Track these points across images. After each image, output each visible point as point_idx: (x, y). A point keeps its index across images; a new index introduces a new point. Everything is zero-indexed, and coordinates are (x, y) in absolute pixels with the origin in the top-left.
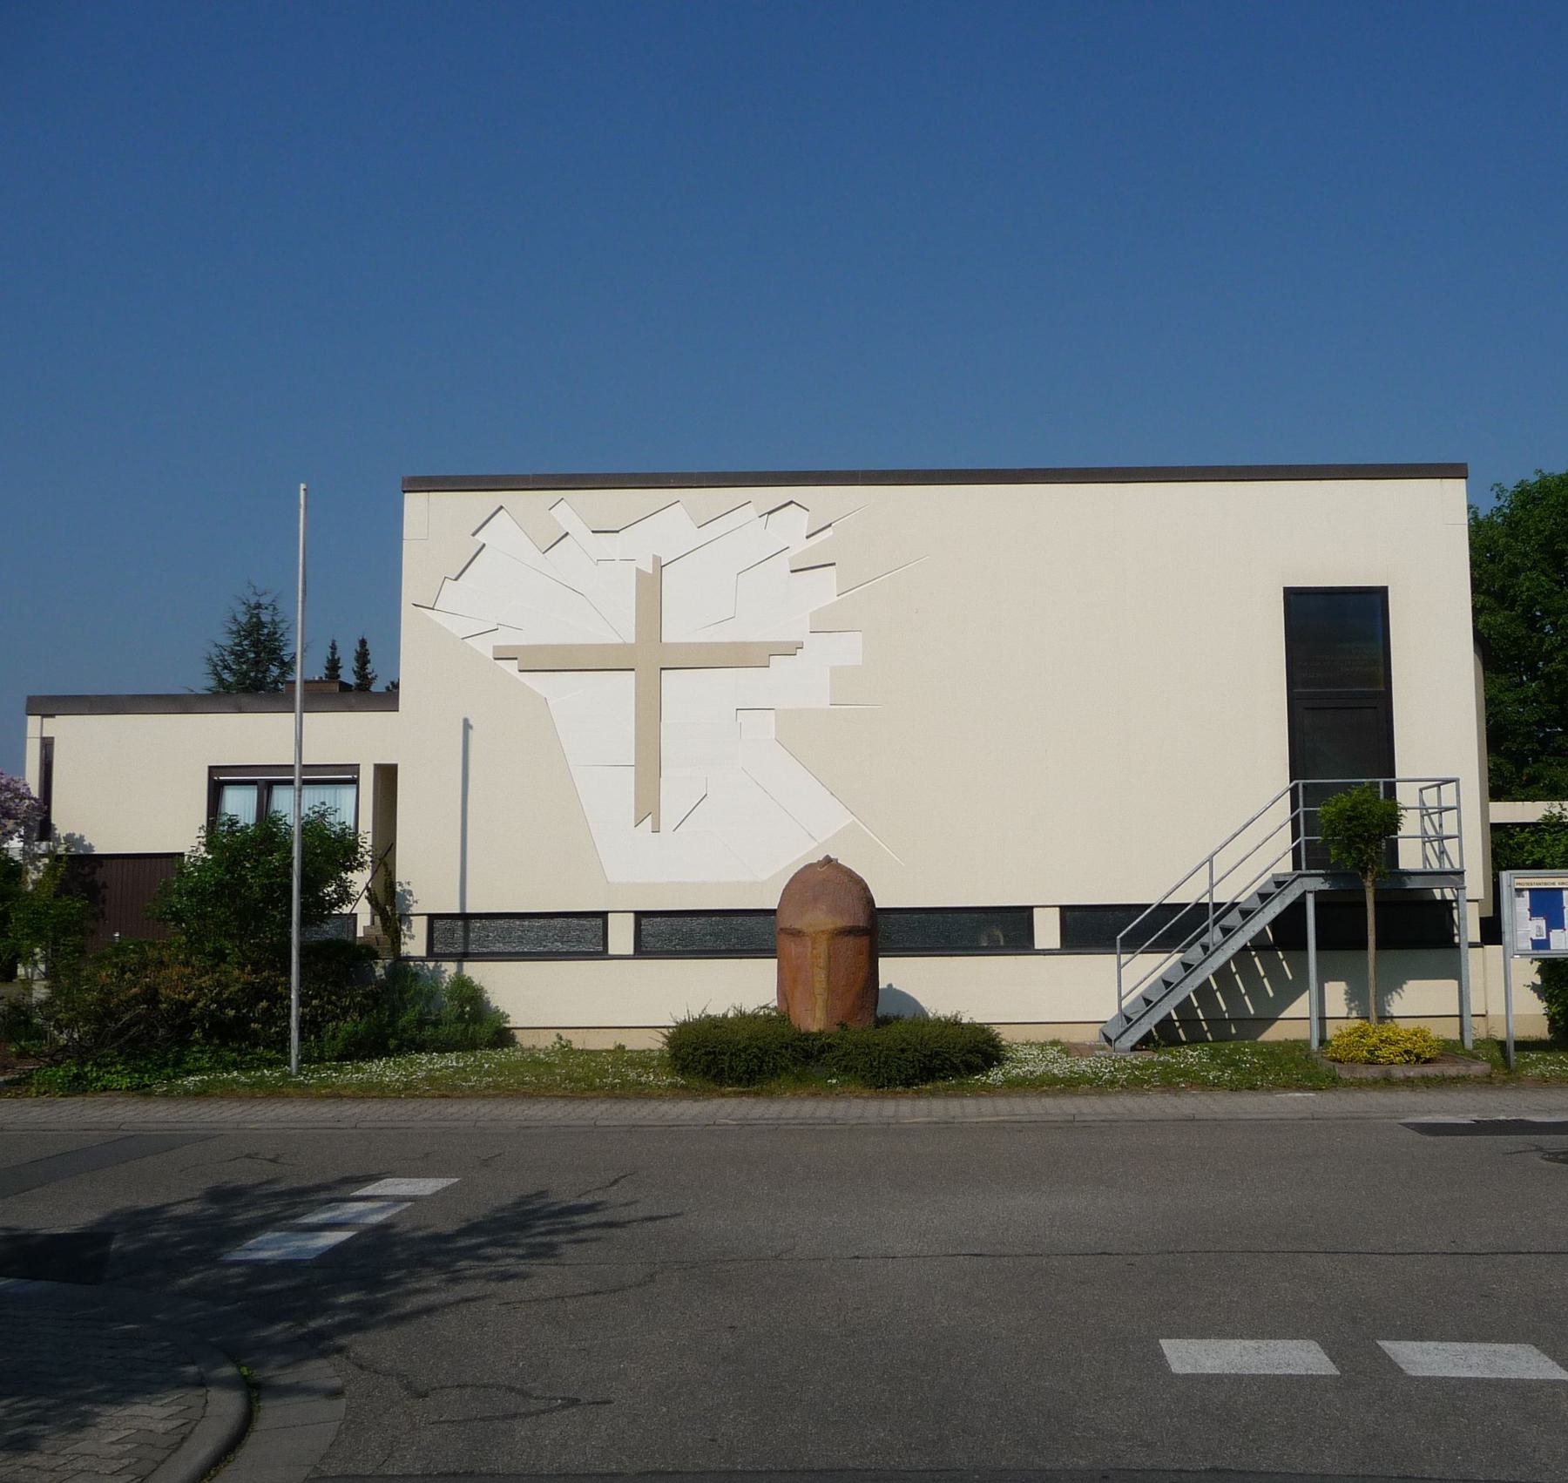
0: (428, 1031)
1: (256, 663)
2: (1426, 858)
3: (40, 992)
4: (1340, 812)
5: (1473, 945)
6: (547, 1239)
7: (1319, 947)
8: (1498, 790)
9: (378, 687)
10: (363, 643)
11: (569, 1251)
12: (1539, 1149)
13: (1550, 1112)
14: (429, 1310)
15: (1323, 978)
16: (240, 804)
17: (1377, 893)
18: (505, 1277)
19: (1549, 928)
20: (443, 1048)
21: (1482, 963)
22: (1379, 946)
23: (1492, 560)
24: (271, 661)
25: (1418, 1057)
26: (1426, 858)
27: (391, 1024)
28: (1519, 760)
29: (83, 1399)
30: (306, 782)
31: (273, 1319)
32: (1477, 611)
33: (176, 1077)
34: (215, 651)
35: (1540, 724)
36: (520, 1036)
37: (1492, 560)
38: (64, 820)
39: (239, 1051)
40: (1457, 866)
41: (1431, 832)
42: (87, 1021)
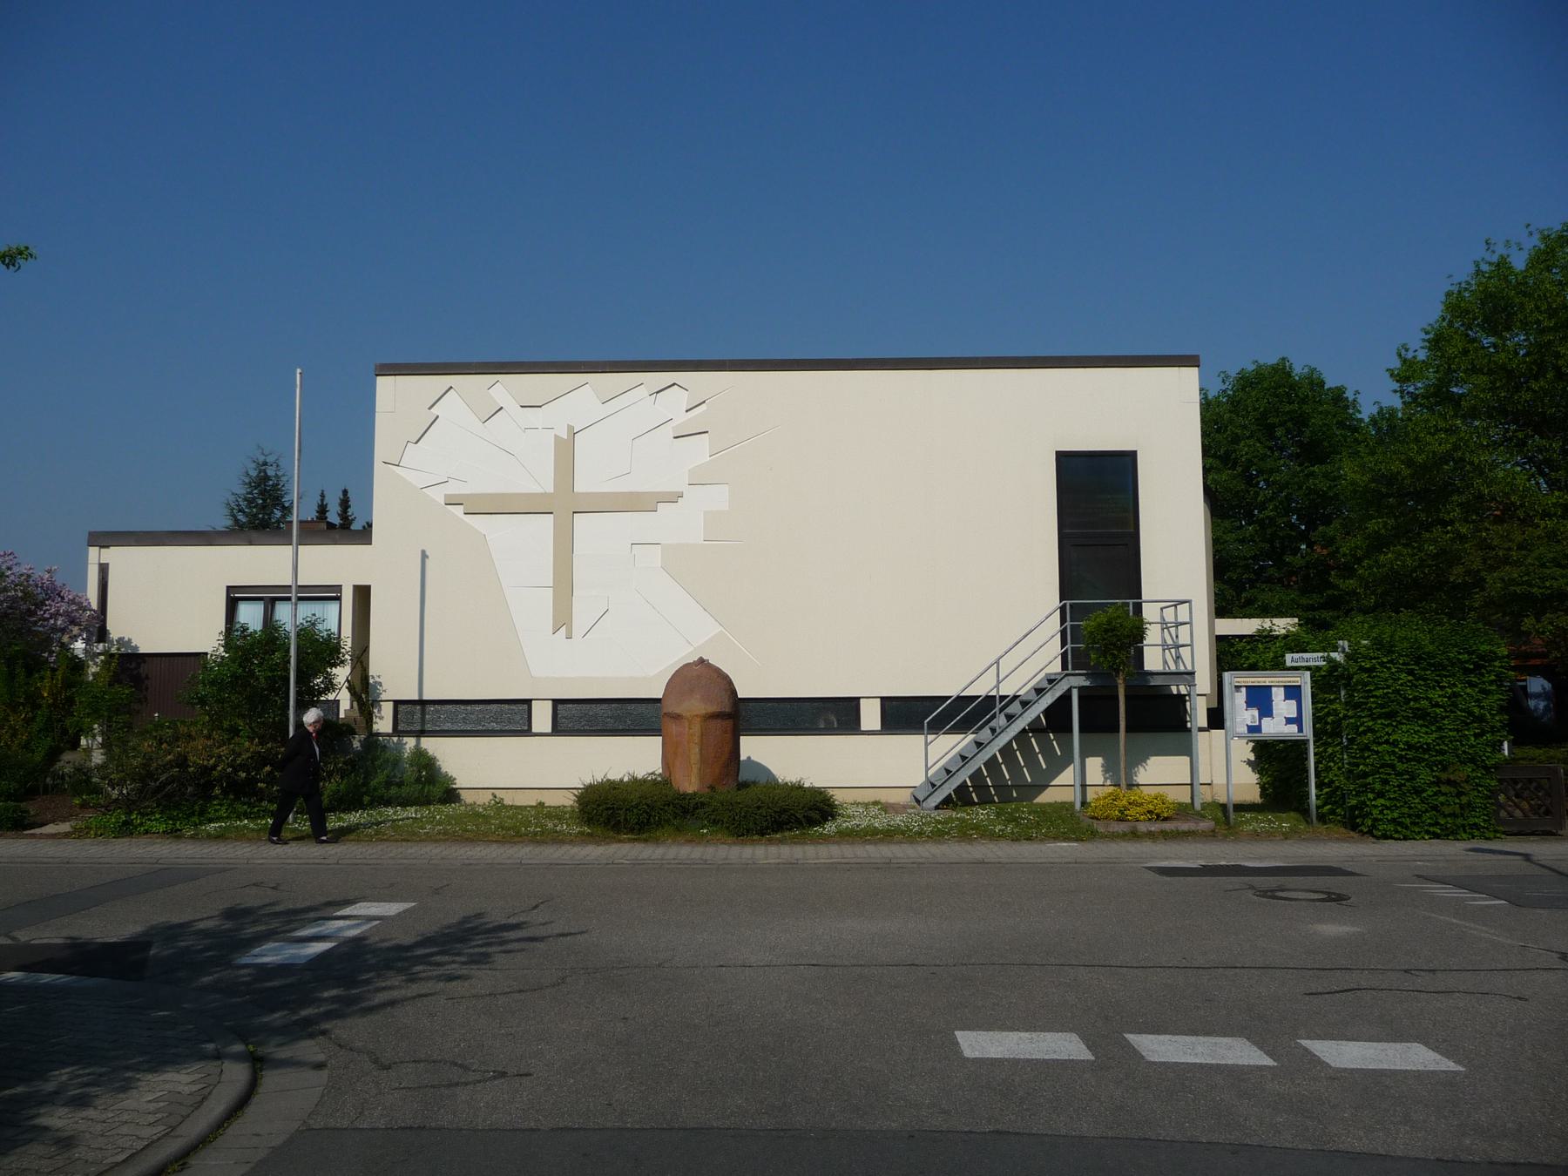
0: (393, 791)
1: (264, 507)
2: (1165, 662)
3: (98, 758)
4: (1099, 625)
5: (1201, 729)
6: (483, 950)
7: (1081, 730)
8: (1223, 607)
9: (356, 526)
10: (345, 492)
11: (501, 959)
12: (1252, 887)
13: (1261, 859)
14: (392, 1003)
15: (1085, 754)
16: (251, 616)
17: (1127, 688)
18: (451, 978)
19: (1261, 716)
20: (405, 803)
21: (1208, 744)
22: (1128, 730)
23: (1218, 431)
24: (275, 506)
25: (1158, 816)
26: (1165, 662)
27: (365, 784)
28: (1239, 587)
29: (127, 1068)
30: (300, 599)
31: (273, 1011)
32: (1206, 471)
33: (201, 824)
34: (232, 498)
35: (1255, 558)
36: (464, 795)
37: (1218, 431)
38: (116, 628)
39: (250, 805)
40: (1189, 668)
41: (1169, 642)
42: (133, 780)
